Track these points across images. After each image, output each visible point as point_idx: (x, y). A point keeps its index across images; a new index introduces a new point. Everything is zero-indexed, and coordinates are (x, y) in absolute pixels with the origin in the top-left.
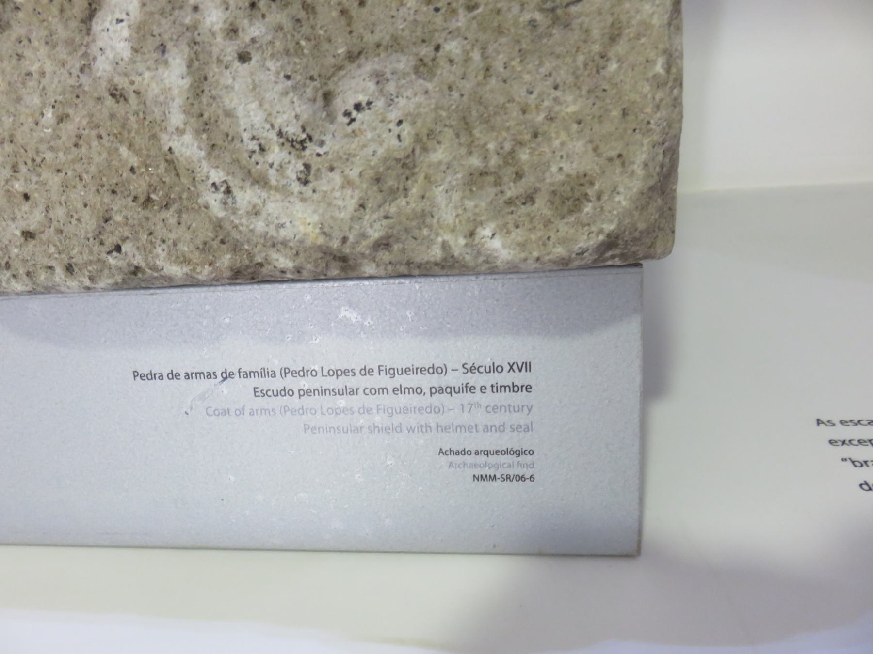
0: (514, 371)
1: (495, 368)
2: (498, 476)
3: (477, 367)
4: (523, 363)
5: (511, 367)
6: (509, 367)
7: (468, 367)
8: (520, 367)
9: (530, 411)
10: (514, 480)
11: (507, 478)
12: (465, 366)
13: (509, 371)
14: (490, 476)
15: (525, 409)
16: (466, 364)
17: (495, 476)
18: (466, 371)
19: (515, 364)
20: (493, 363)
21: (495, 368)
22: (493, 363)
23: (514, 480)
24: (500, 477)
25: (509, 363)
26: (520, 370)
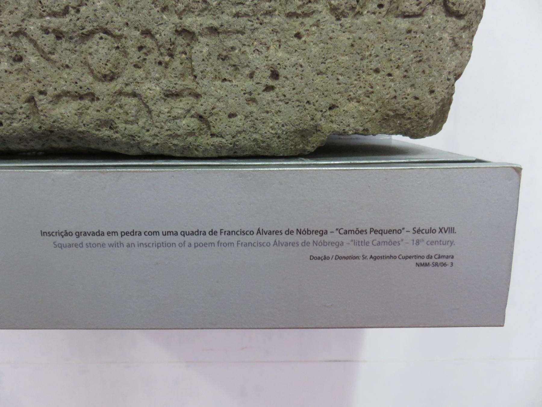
0: (442, 233)
1: (432, 231)
2: (431, 263)
3: (421, 230)
4: (448, 228)
5: (441, 230)
6: (439, 230)
7: (416, 230)
8: (446, 230)
9: (452, 244)
10: (440, 266)
11: (436, 265)
12: (415, 229)
13: (439, 233)
15: (449, 243)
16: (415, 228)
17: (429, 263)
18: (414, 232)
19: (443, 229)
20: (431, 228)
21: (432, 231)
22: (431, 228)
23: (440, 266)
24: (431, 264)
25: (440, 228)
26: (446, 232)
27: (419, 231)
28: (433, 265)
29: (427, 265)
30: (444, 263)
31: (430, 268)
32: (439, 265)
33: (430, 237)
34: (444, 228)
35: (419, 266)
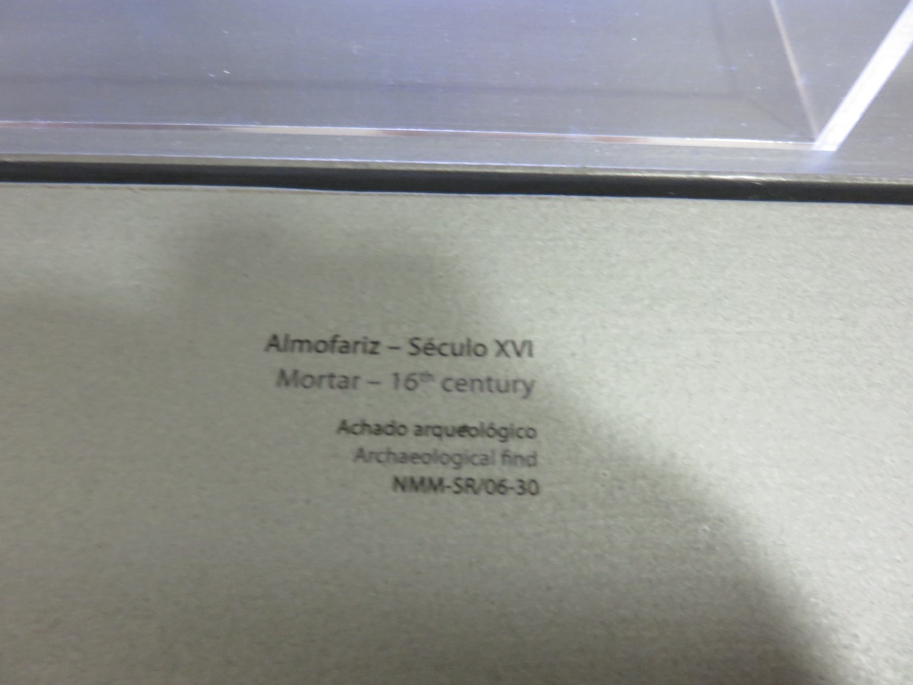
0: (507, 355)
5: (502, 347)
6: (496, 348)
12: (416, 342)
14: (431, 481)
18: (413, 350)
26: (519, 354)
27: (429, 349)
28: (456, 489)
29: (437, 485)
30: (497, 480)
31: (446, 497)
32: (480, 489)
34: (513, 343)
35: (403, 488)
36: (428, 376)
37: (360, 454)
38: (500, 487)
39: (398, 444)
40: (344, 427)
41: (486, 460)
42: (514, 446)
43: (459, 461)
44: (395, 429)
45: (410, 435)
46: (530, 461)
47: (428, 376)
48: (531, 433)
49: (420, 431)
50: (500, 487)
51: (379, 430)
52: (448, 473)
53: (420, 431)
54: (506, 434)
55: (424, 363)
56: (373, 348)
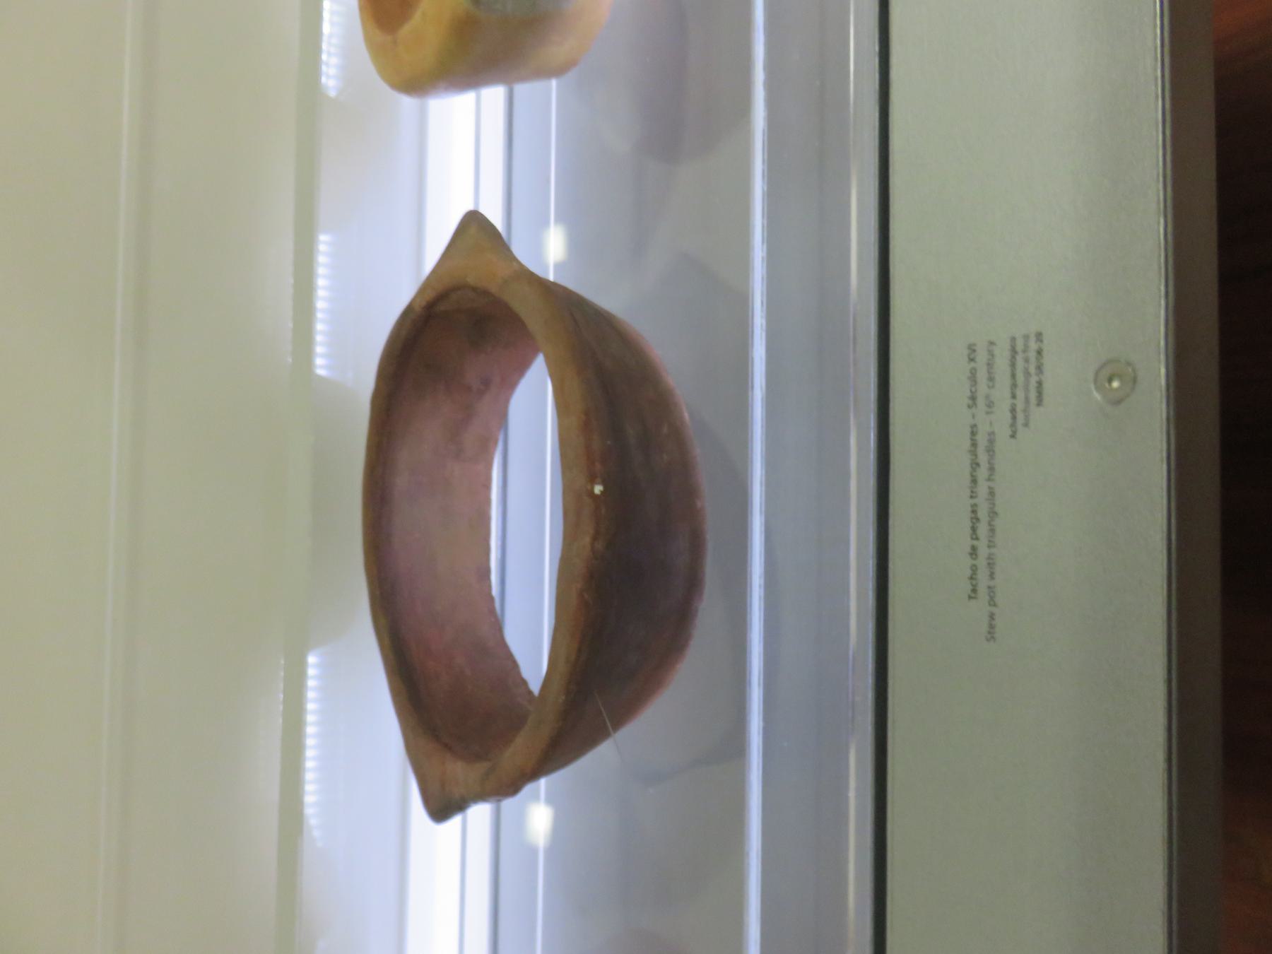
5: (972, 360)
7: (970, 402)
27: (973, 398)
29: (1040, 384)
33: (982, 375)
36: (987, 397)
37: (1026, 425)
38: (1039, 352)
39: (1020, 406)
40: (1013, 436)
41: (1027, 360)
42: (1020, 347)
43: (1027, 374)
44: (1013, 410)
45: (1015, 402)
46: (1026, 337)
47: (987, 397)
48: (1013, 339)
49: (1014, 397)
50: (1039, 352)
51: (1014, 418)
52: (1034, 380)
53: (1014, 397)
54: (1014, 351)
55: (981, 402)
56: (974, 426)
